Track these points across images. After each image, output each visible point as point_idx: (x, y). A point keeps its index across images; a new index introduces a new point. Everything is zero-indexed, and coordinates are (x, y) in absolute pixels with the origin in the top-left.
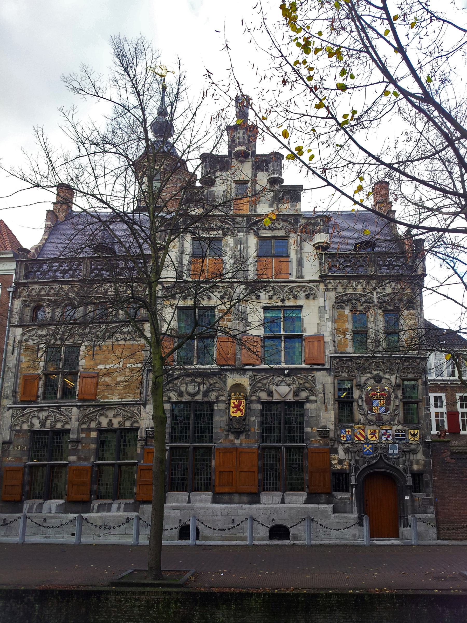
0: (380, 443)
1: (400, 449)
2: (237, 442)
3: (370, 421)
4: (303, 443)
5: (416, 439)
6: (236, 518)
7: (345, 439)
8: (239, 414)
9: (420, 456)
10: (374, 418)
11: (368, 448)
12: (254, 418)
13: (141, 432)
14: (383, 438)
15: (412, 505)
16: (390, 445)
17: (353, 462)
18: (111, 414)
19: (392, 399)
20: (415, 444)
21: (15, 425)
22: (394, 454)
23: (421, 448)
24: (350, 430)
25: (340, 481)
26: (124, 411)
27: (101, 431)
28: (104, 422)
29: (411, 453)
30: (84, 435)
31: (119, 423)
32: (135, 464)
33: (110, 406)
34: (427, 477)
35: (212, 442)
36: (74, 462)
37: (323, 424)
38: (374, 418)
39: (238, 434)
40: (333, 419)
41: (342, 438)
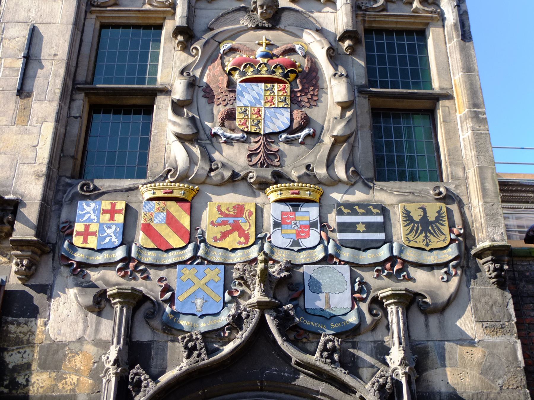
5: (435, 242)
7: (93, 242)
20: (431, 267)
41: (77, 241)
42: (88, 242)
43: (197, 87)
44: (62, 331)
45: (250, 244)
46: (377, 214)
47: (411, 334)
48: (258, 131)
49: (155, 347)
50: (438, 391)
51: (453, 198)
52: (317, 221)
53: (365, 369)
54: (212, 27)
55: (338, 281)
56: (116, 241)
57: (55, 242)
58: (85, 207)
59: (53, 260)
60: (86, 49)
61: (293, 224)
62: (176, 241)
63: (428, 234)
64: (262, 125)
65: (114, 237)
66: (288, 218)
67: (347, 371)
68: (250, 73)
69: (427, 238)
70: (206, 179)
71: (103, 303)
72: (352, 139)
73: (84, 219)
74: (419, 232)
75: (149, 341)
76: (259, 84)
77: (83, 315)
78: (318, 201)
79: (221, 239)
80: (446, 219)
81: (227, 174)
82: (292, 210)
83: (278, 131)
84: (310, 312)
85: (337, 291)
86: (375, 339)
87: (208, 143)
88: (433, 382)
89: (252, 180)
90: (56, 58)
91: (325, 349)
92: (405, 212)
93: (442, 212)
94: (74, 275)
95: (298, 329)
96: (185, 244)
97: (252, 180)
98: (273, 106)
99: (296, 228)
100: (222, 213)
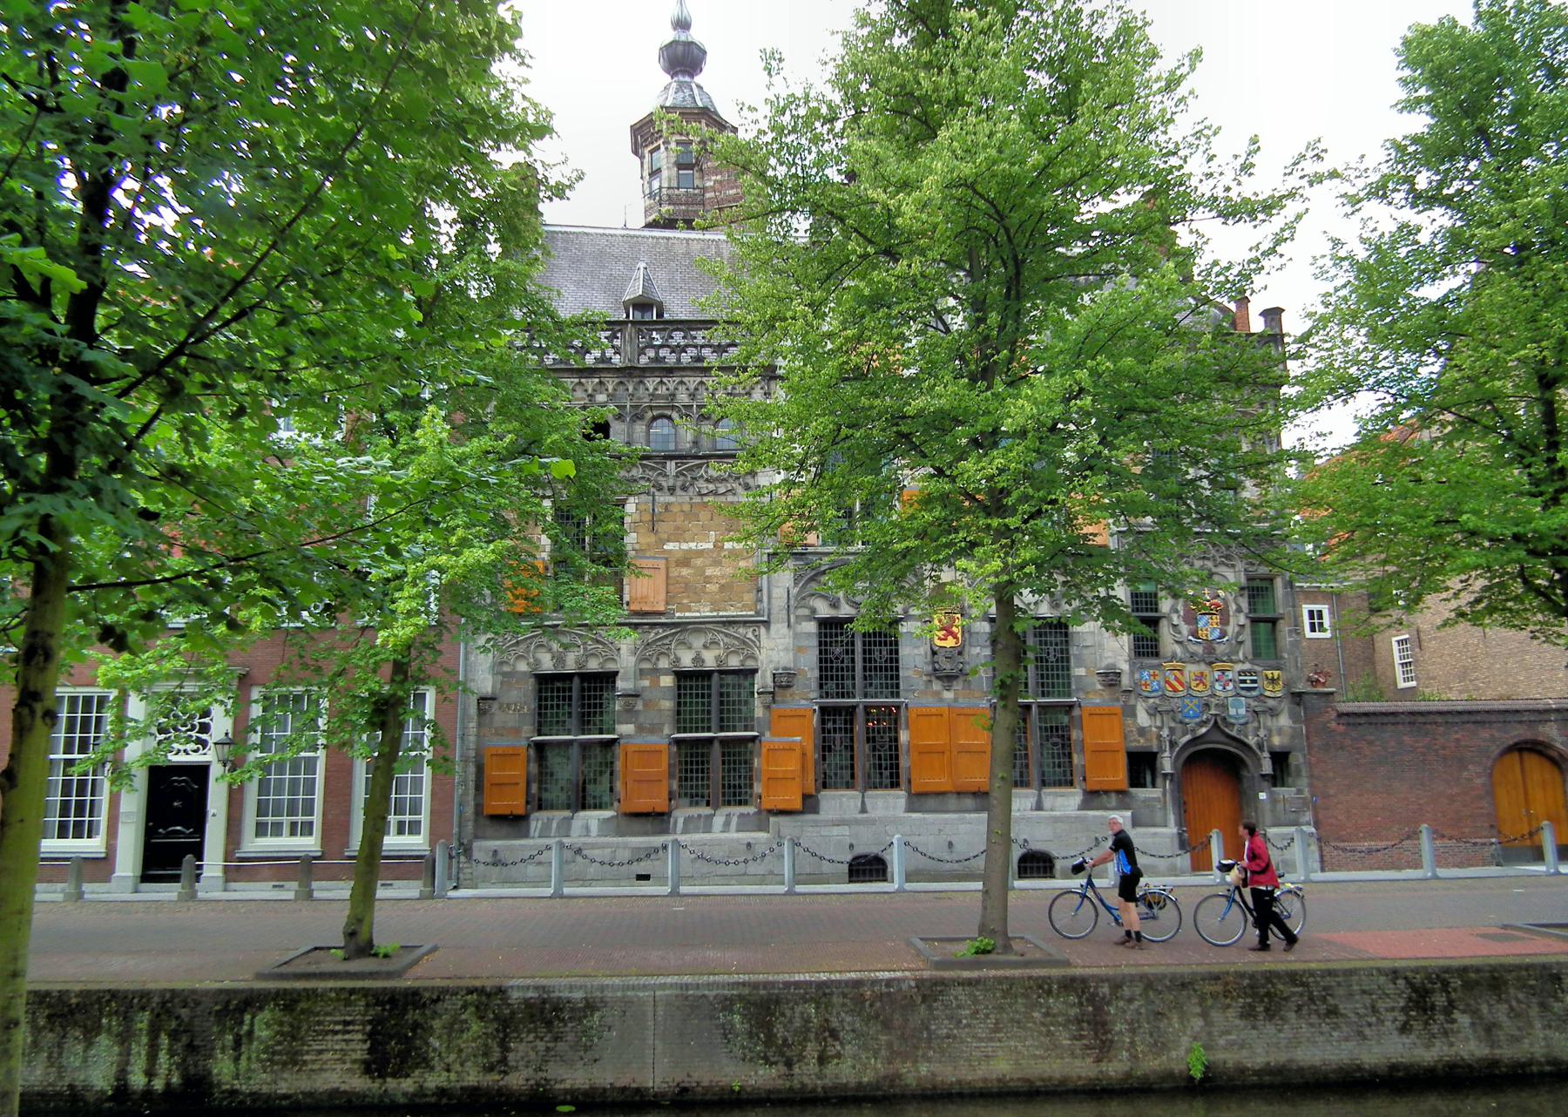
1: (1248, 706)
2: (948, 695)
3: (1193, 655)
4: (1069, 696)
6: (955, 840)
8: (950, 642)
9: (1284, 721)
10: (1199, 650)
11: (1192, 706)
12: (978, 650)
13: (763, 677)
14: (1218, 687)
15: (1273, 811)
17: (1165, 733)
18: (698, 642)
21: (502, 663)
23: (1285, 706)
25: (1141, 765)
26: (727, 635)
27: (681, 675)
28: (687, 661)
30: (646, 683)
31: (717, 658)
32: (753, 739)
33: (698, 626)
34: (1296, 759)
35: (898, 696)
36: (629, 736)
37: (1110, 661)
38: (1199, 650)
39: (948, 679)
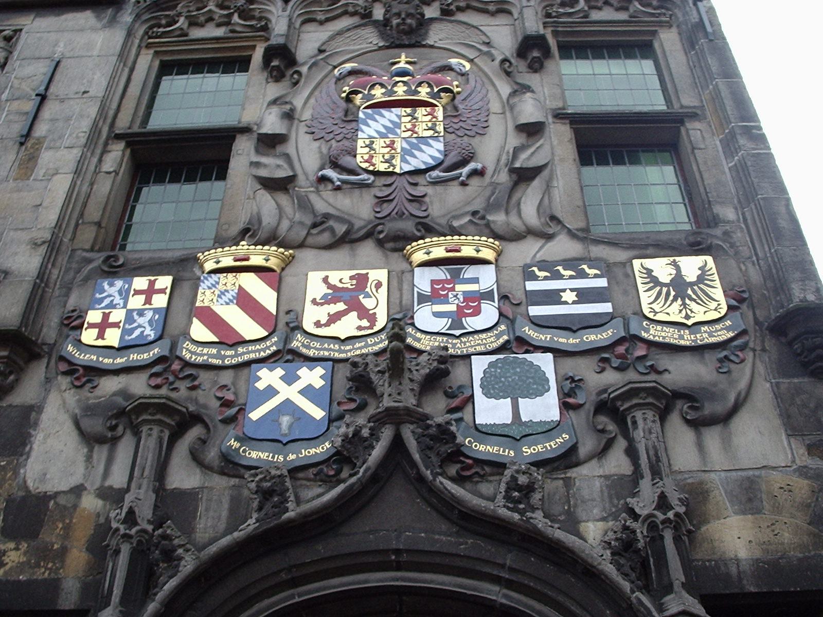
0: (398, 353)
7: (113, 337)
9: (759, 441)
11: (291, 394)
16: (480, 365)
19: (495, 106)
22: (517, 433)
24: (164, 282)
29: (675, 420)
40: (51, 216)
42: (105, 337)
43: (296, 122)
44: (48, 476)
45: (376, 329)
46: (596, 276)
47: (672, 462)
48: (391, 169)
49: (204, 498)
50: (733, 556)
51: (724, 249)
52: (493, 289)
53: (591, 525)
54: (323, 48)
55: (532, 378)
56: (151, 334)
57: (52, 342)
58: (106, 286)
59: (47, 367)
60: (134, 89)
61: (450, 295)
62: (249, 329)
63: (687, 301)
64: (397, 161)
65: (148, 328)
66: (443, 289)
67: (556, 526)
68: (378, 93)
69: (685, 308)
70: (305, 238)
71: (120, 429)
72: (545, 173)
73: (103, 305)
74: (671, 298)
75: (194, 488)
76: (393, 109)
77: (86, 450)
78: (493, 261)
79: (328, 324)
80: (716, 277)
81: (341, 229)
82: (449, 277)
83: (423, 167)
84: (483, 430)
85: (532, 394)
86: (607, 473)
87: (310, 191)
88: (723, 542)
89: (381, 236)
90: (85, 95)
91: (513, 485)
92: (645, 271)
93: (707, 268)
94: (77, 387)
95: (462, 458)
96: (266, 334)
97: (381, 236)
98: (415, 135)
99: (456, 302)
100: (330, 286)
